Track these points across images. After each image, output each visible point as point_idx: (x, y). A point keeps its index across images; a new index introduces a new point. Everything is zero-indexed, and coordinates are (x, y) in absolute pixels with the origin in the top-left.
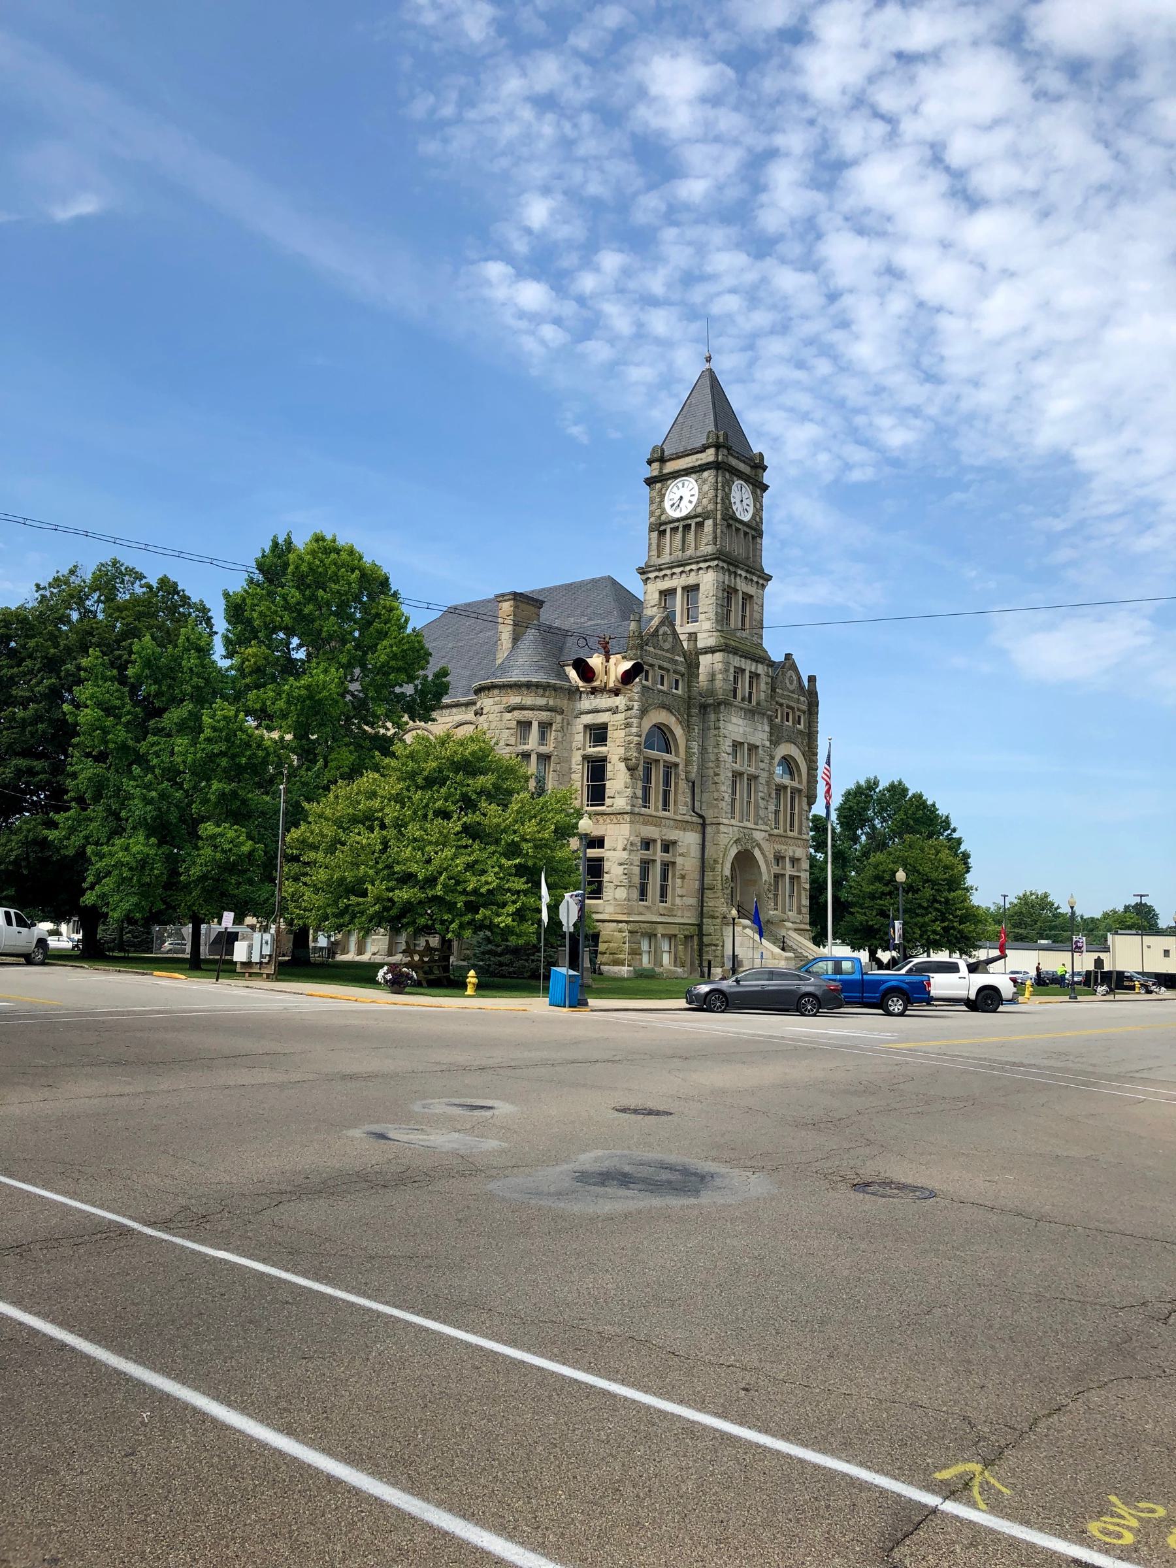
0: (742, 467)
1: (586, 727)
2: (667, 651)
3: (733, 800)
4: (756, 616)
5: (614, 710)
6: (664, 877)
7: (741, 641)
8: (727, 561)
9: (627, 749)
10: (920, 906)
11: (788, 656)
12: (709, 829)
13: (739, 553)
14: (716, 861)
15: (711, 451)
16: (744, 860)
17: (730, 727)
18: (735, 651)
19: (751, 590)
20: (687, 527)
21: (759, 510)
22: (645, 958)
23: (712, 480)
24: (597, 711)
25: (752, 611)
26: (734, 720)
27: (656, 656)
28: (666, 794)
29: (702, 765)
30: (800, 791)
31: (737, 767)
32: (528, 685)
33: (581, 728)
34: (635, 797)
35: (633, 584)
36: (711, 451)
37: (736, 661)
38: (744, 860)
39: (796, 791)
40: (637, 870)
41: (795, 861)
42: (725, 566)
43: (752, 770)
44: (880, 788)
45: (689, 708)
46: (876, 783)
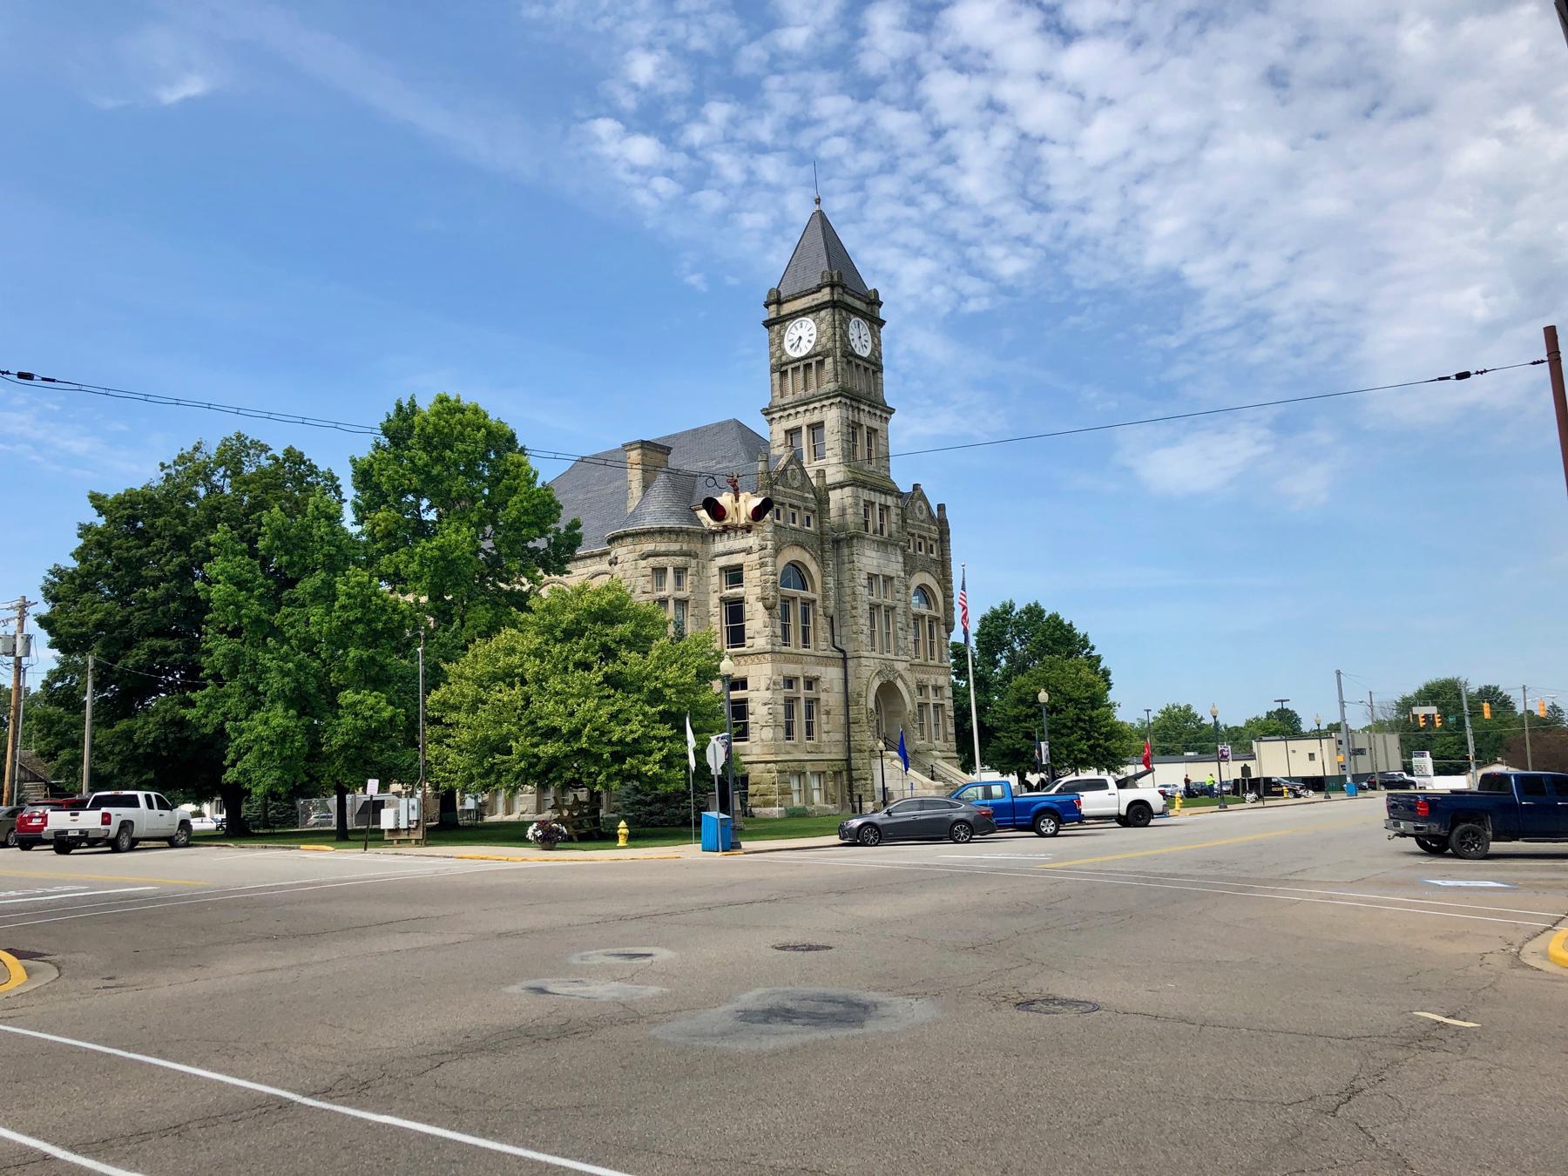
0: (858, 304)
1: (721, 569)
3: (873, 633)
4: (882, 448)
5: (748, 551)
6: (809, 714)
7: (869, 477)
8: (850, 398)
9: (764, 589)
10: (1065, 726)
11: (916, 487)
12: (850, 663)
13: (860, 388)
14: (859, 695)
15: (827, 290)
16: (888, 691)
17: (864, 560)
18: (864, 485)
19: (875, 424)
20: (808, 366)
21: (877, 346)
22: (796, 797)
23: (829, 318)
24: (732, 553)
25: (877, 445)
26: (868, 553)
27: (785, 495)
28: (805, 631)
29: (839, 600)
30: (938, 619)
31: (874, 599)
32: (661, 532)
33: (716, 571)
34: (774, 635)
35: (759, 426)
36: (827, 290)
37: (866, 495)
38: (888, 691)
39: (933, 620)
40: (781, 709)
41: (937, 689)
43: (889, 602)
44: (1017, 609)
45: (822, 543)
46: (1012, 607)
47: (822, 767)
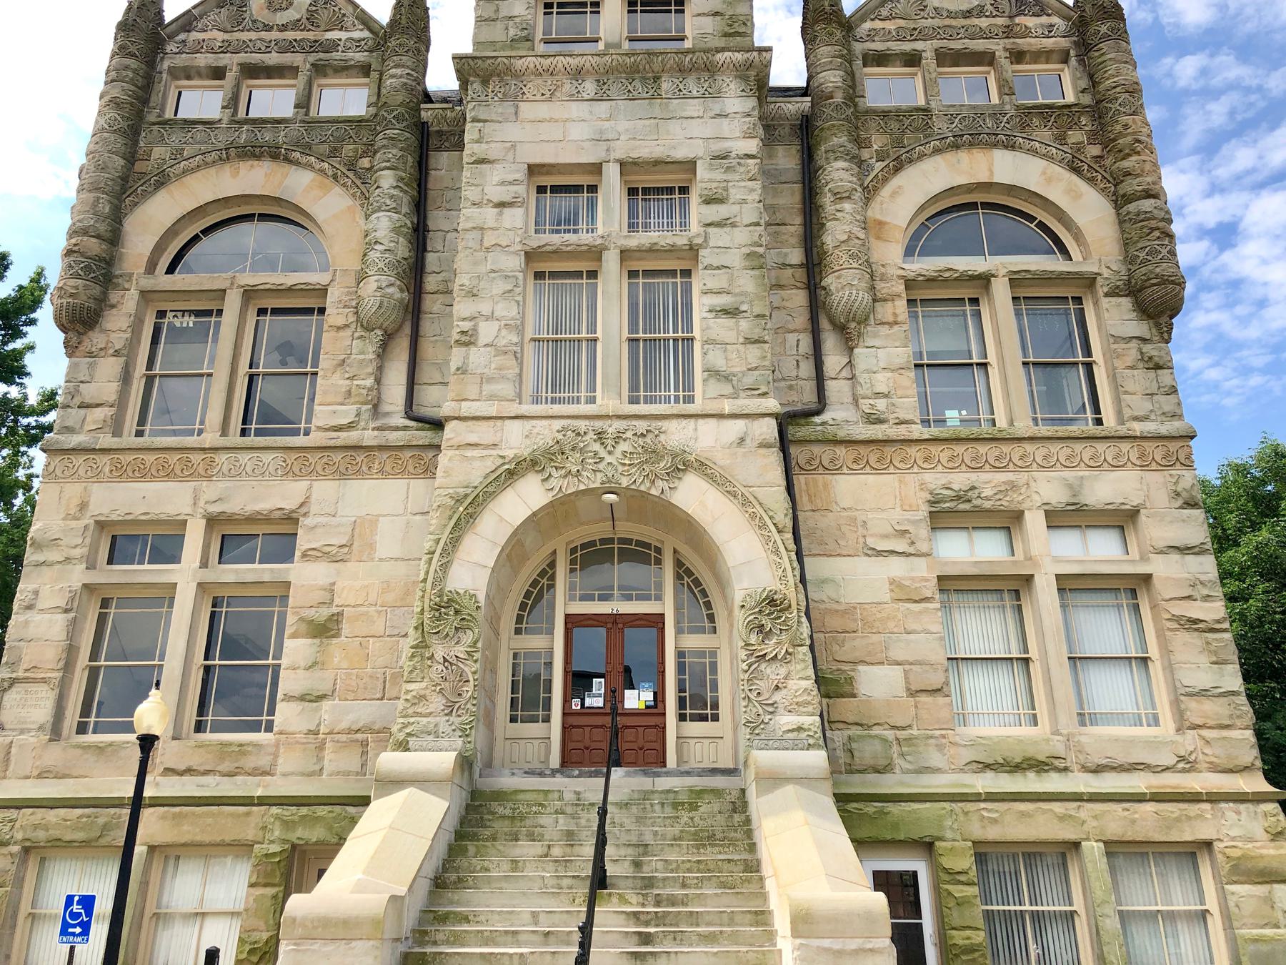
2: (283, 28)
27: (225, 48)
30: (1089, 281)
47: (248, 825)
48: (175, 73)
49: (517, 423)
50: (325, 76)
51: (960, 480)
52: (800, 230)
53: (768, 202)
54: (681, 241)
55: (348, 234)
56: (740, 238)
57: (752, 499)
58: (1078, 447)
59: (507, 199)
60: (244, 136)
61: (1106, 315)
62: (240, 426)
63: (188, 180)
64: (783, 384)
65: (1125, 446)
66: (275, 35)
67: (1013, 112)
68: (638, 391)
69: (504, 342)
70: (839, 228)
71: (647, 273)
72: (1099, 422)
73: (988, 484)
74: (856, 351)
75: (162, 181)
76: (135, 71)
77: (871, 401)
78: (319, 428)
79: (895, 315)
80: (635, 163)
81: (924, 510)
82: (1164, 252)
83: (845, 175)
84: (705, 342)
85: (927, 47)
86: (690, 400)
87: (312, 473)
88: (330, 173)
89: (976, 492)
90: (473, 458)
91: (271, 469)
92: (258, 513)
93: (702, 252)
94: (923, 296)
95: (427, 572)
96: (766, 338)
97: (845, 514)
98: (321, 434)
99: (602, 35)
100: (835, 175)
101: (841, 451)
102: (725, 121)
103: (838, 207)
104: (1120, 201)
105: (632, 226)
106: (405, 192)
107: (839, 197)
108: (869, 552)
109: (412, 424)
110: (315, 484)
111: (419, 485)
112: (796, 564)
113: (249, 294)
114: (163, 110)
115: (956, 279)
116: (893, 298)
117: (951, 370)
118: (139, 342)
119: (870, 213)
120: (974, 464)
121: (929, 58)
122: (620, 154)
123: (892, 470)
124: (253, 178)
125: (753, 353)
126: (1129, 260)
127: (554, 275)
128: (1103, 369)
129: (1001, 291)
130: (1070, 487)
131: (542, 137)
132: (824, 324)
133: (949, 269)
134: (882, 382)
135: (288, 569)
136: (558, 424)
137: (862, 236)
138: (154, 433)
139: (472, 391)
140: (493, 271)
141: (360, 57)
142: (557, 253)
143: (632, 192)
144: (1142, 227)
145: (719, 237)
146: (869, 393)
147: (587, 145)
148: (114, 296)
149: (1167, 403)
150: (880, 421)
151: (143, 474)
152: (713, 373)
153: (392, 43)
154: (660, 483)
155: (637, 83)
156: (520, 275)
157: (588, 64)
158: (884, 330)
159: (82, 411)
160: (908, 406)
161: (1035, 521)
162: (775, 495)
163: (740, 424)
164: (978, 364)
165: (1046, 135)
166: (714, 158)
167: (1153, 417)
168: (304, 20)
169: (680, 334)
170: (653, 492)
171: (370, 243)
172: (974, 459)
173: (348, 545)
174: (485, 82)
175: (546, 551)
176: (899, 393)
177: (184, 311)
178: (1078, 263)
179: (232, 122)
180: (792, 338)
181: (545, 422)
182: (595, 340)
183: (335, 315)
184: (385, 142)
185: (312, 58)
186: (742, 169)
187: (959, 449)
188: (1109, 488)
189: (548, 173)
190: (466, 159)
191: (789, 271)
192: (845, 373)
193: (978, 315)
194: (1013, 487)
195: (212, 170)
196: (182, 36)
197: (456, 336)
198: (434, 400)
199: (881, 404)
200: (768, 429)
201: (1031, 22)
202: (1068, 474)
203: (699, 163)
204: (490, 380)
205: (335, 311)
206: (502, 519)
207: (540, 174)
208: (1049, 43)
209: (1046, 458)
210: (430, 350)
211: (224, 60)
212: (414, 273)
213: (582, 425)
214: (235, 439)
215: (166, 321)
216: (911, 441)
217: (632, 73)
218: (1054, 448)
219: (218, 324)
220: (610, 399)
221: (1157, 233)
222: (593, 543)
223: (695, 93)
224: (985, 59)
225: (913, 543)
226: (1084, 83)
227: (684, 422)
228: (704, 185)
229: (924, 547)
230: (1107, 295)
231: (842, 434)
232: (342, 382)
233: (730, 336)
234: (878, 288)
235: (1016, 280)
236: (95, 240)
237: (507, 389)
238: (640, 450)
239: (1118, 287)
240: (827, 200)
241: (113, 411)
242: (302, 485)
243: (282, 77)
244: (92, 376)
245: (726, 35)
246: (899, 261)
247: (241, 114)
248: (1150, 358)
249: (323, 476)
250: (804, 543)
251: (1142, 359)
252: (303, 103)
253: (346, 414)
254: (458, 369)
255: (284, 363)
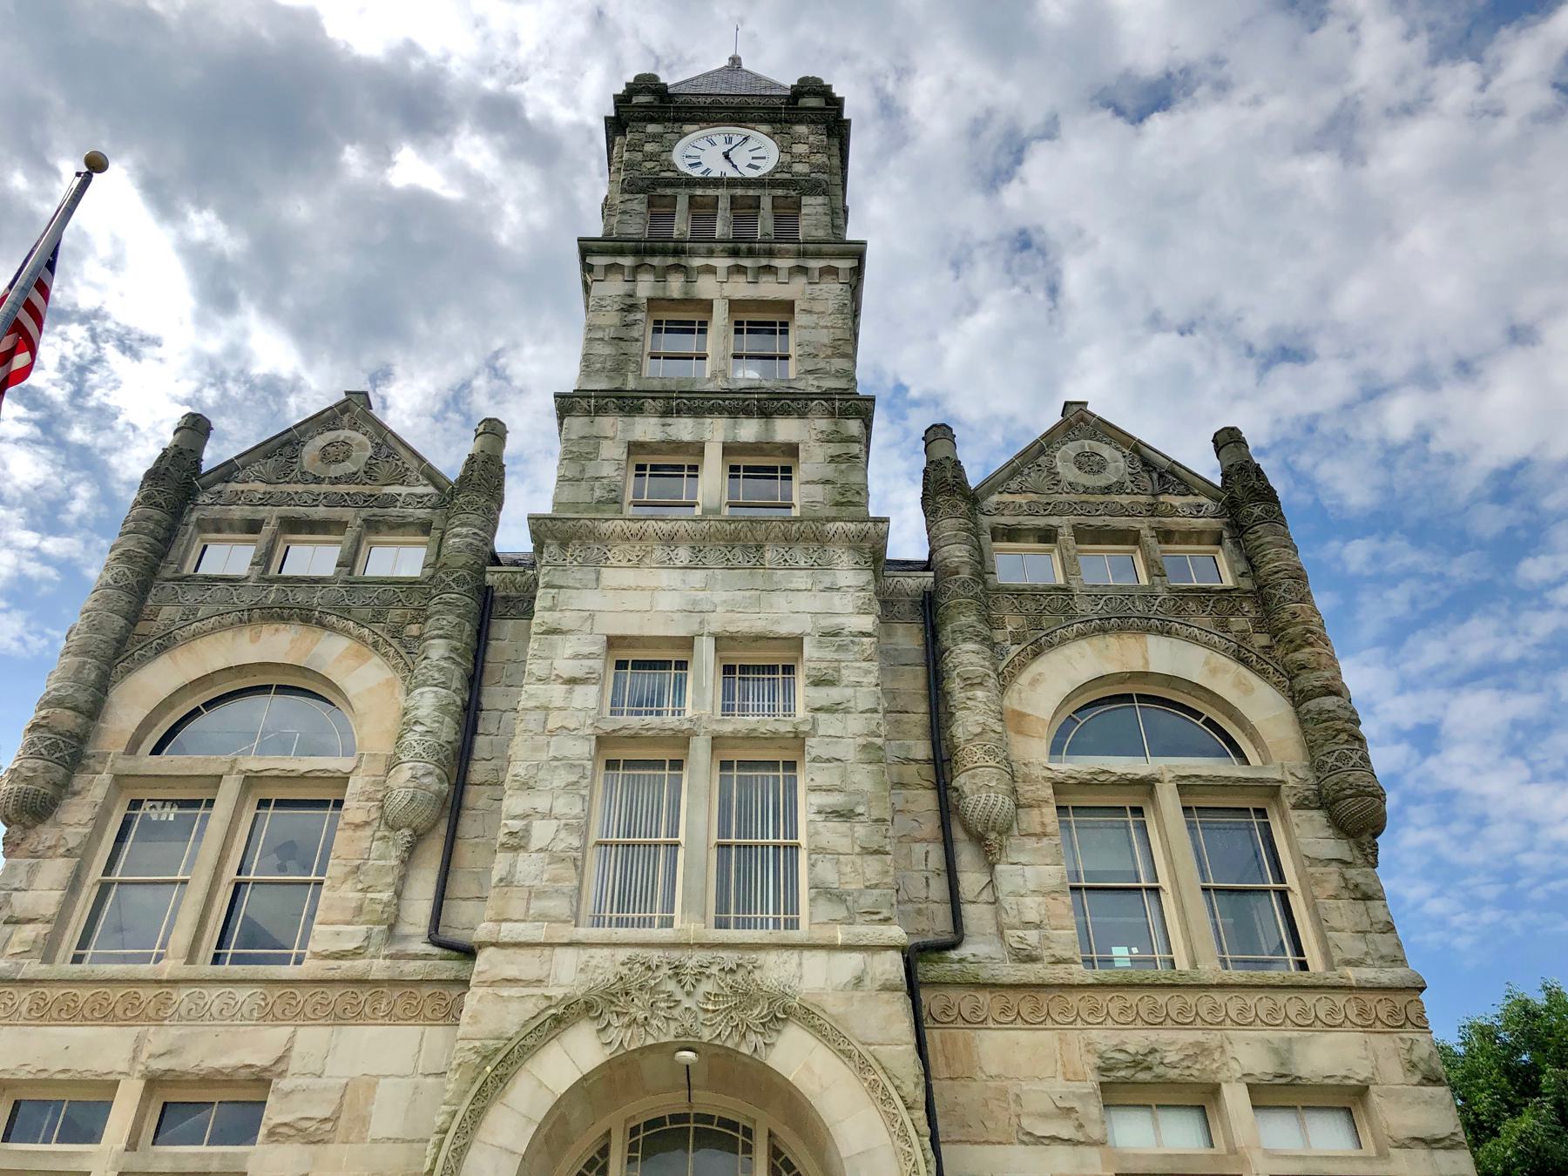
2: (336, 481)
18: (627, 403)
19: (769, 289)
30: (1273, 790)
37: (647, 428)
42: (627, 261)
48: (202, 526)
49: (570, 951)
50: (378, 533)
51: (1137, 1040)
52: (926, 718)
53: (888, 685)
54: (785, 728)
55: (382, 707)
56: (856, 723)
57: (872, 1061)
58: (1281, 998)
59: (579, 674)
60: (273, 596)
61: (1297, 831)
62: (213, 950)
63: (201, 645)
64: (909, 907)
65: (1340, 999)
66: (326, 487)
67: (1165, 595)
68: (727, 912)
69: (562, 846)
70: (971, 718)
71: (743, 764)
72: (1303, 966)
73: (1173, 1045)
74: (998, 867)
75: (166, 643)
76: (158, 523)
77: (1020, 933)
78: (316, 955)
79: (1043, 824)
80: (732, 638)
81: (1093, 1080)
82: (1356, 757)
83: (974, 658)
84: (812, 852)
85: (1064, 523)
86: (793, 924)
87: (299, 1017)
88: (370, 640)
89: (1158, 1055)
90: (510, 998)
91: (245, 1009)
92: (219, 1071)
93: (809, 742)
94: (1077, 802)
95: (435, 1160)
96: (888, 848)
97: (991, 1084)
98: (316, 962)
99: (699, 500)
100: (965, 658)
101: (984, 997)
102: (836, 596)
103: (969, 694)
104: (1298, 698)
105: (727, 709)
106: (459, 664)
107: (970, 683)
108: (1025, 1138)
109: (436, 951)
110: (301, 1031)
111: (436, 1035)
112: (930, 1154)
113: (251, 781)
114: (182, 565)
115: (1113, 783)
116: (1039, 804)
117: (1114, 895)
118: (100, 837)
119: (1006, 702)
120: (1151, 1019)
121: (1066, 534)
122: (715, 627)
123: (1049, 1024)
124: (278, 644)
125: (872, 868)
126: (1317, 766)
127: (630, 764)
128: (1300, 897)
129: (1169, 799)
130: (1276, 1051)
131: (625, 607)
132: (958, 833)
133: (1104, 772)
134: (1032, 908)
135: (247, 1154)
136: (623, 954)
137: (999, 729)
138: (97, 959)
139: (516, 907)
140: (555, 759)
141: (422, 513)
142: (635, 738)
143: (728, 670)
144: (1326, 729)
145: (829, 725)
146: (1016, 921)
147: (677, 616)
148: (79, 781)
149: (1384, 944)
150: (1032, 959)
151: (72, 1014)
152: (822, 891)
153: (461, 499)
154: (752, 1037)
155: (737, 551)
156: (589, 765)
157: (682, 530)
158: (1031, 843)
159: (8, 929)
160: (1065, 939)
161: (1236, 1099)
162: (902, 1056)
163: (855, 960)
164: (1147, 889)
165: (1206, 621)
166: (824, 635)
167: (1369, 961)
168: (361, 473)
169: (782, 840)
170: (744, 1049)
171: (408, 721)
172: (1152, 1012)
173: (333, 1119)
174: (564, 545)
175: (597, 1131)
176: (1053, 922)
177: (165, 801)
178: (1256, 768)
179: (261, 579)
180: (919, 849)
181: (606, 952)
182: (677, 845)
183: (354, 810)
184: (440, 607)
185: (365, 513)
186: (856, 648)
187: (1133, 998)
188: (1328, 1054)
189: (629, 647)
190: (534, 629)
191: (914, 767)
192: (985, 896)
193: (1143, 827)
194: (1203, 1050)
195: (229, 634)
196: (218, 487)
197: (502, 838)
198: (472, 919)
199: (1032, 936)
200: (891, 966)
201: (1177, 501)
202: (1270, 1034)
203: (806, 640)
204: (541, 894)
205: (355, 804)
206: (541, 1084)
207: (620, 647)
208: (1199, 523)
209: (1241, 1012)
210: (470, 855)
211: (263, 512)
212: (459, 760)
213: (655, 956)
214: (204, 968)
215: (140, 812)
216: (1072, 986)
217: (732, 541)
218: (1252, 999)
219: (206, 818)
220: (690, 923)
221: (1344, 736)
222: (660, 1121)
223: (802, 564)
224: (1131, 537)
225: (1081, 1126)
226: (1242, 566)
227: (786, 954)
228: (812, 665)
229: (1095, 1132)
230: (1295, 807)
231: (985, 975)
232: (351, 895)
233: (843, 844)
234: (1020, 791)
235: (1185, 787)
236: (68, 712)
237: (559, 906)
238: (727, 991)
239: (1306, 798)
240: (955, 686)
241: (47, 928)
242: (284, 1032)
243: (326, 533)
244: (30, 883)
245: (838, 504)
246: (1044, 759)
247: (273, 571)
248: (1356, 886)
249: (312, 1020)
250: (941, 1124)
251: (1346, 887)
252: (348, 562)
253: (353, 935)
254: (501, 880)
255: (282, 869)
